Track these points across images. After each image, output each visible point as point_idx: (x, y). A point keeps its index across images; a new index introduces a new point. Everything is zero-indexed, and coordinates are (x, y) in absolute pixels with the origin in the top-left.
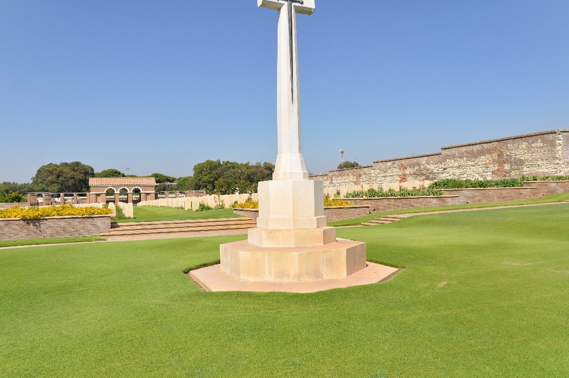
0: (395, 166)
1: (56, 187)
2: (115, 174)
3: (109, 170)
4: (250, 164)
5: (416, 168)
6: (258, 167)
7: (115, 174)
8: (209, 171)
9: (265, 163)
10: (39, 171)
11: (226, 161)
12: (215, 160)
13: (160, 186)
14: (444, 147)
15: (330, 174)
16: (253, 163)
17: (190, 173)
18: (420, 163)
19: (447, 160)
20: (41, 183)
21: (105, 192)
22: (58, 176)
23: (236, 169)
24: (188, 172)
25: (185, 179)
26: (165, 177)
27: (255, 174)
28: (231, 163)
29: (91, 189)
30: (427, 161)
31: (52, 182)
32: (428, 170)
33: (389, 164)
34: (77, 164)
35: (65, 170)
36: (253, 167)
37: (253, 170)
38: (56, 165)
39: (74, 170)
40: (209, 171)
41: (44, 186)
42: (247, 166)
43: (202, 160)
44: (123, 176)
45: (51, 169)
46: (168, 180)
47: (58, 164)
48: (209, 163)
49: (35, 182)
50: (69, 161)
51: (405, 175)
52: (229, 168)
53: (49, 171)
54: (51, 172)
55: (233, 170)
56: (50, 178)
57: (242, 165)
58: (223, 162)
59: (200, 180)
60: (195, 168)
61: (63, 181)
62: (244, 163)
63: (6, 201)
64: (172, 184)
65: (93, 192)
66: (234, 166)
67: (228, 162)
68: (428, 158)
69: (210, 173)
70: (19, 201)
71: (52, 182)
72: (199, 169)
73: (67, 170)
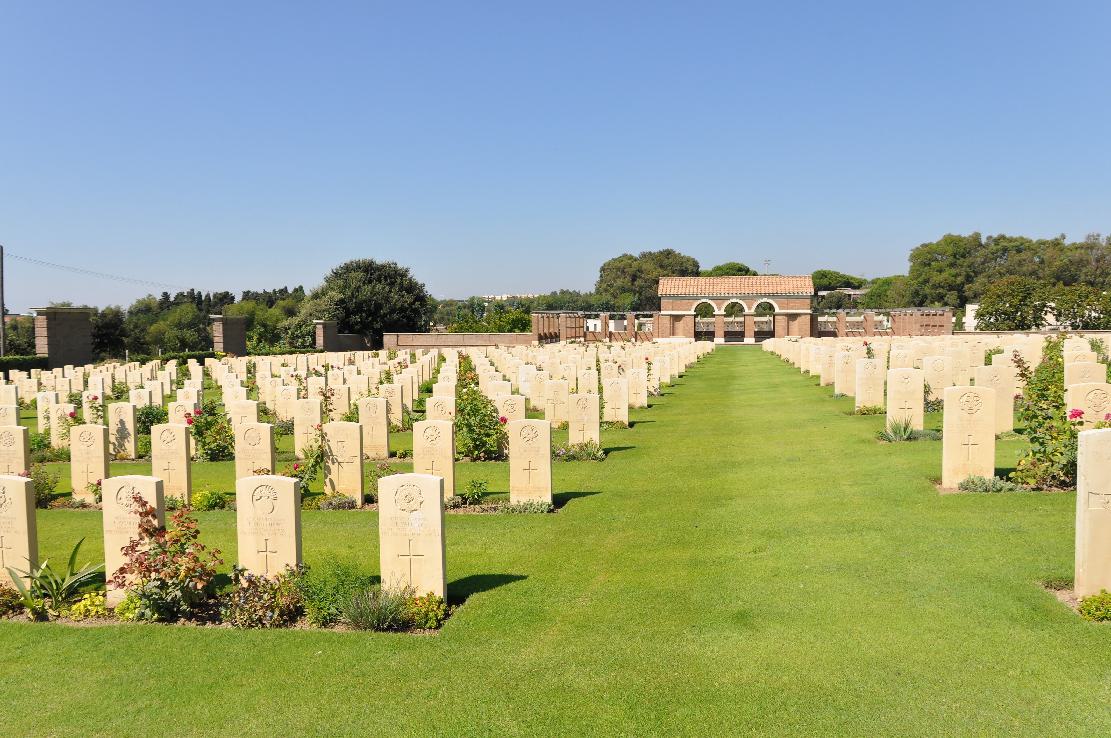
1: (629, 299)
2: (742, 271)
3: (727, 264)
4: (1067, 242)
6: (1090, 246)
7: (742, 271)
8: (951, 259)
10: (603, 269)
11: (995, 236)
12: (966, 232)
13: (831, 296)
16: (1075, 236)
17: (902, 268)
20: (606, 290)
22: (634, 280)
23: (1023, 256)
24: (900, 267)
25: (888, 282)
26: (843, 276)
27: (1082, 263)
28: (1011, 240)
29: (663, 302)
31: (624, 290)
34: (668, 253)
35: (644, 267)
36: (1081, 247)
37: (1077, 254)
38: (631, 257)
39: (661, 266)
40: (951, 259)
41: (609, 297)
42: (1056, 244)
43: (935, 238)
44: (755, 274)
45: (621, 265)
46: (848, 284)
47: (636, 255)
48: (951, 240)
49: (598, 291)
50: (655, 248)
52: (1005, 250)
53: (618, 269)
54: (623, 272)
55: (1017, 258)
56: (619, 282)
57: (1042, 243)
58: (989, 238)
59: (926, 281)
60: (913, 258)
61: (641, 288)
62: (1050, 236)
63: (501, 330)
64: (858, 292)
65: (667, 311)
66: (1021, 247)
67: (1003, 237)
69: (952, 265)
70: (523, 330)
71: (624, 290)
72: (924, 258)
73: (648, 266)
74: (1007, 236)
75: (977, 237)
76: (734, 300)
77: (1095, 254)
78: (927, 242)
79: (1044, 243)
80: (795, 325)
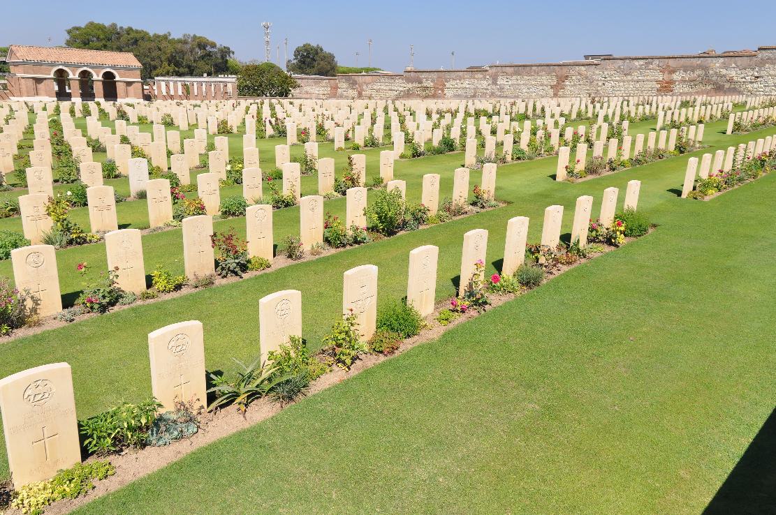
0: (651, 66)
5: (698, 72)
6: (185, 42)
9: (195, 36)
12: (107, 24)
14: (764, 46)
15: (494, 70)
16: (176, 35)
18: (707, 66)
19: (767, 65)
21: (52, 76)
28: (137, 32)
30: (724, 63)
32: (725, 76)
33: (636, 63)
36: (180, 41)
37: (179, 46)
42: (165, 37)
51: (672, 82)
62: (161, 33)
67: (131, 29)
68: (726, 59)
74: (134, 29)
75: (114, 25)
76: (61, 67)
77: (188, 46)
78: (77, 26)
79: (159, 36)
80: (131, 88)
